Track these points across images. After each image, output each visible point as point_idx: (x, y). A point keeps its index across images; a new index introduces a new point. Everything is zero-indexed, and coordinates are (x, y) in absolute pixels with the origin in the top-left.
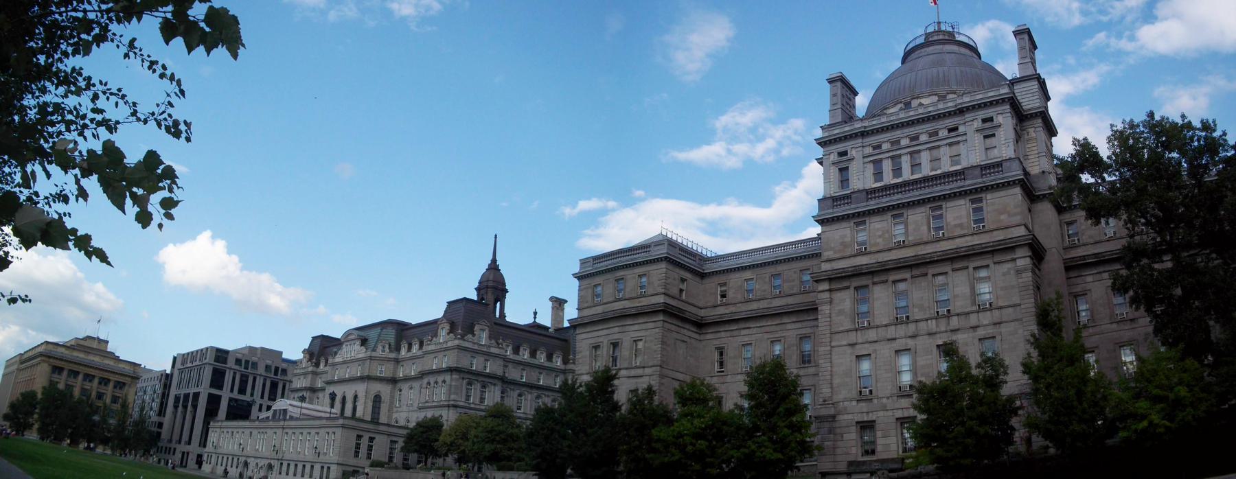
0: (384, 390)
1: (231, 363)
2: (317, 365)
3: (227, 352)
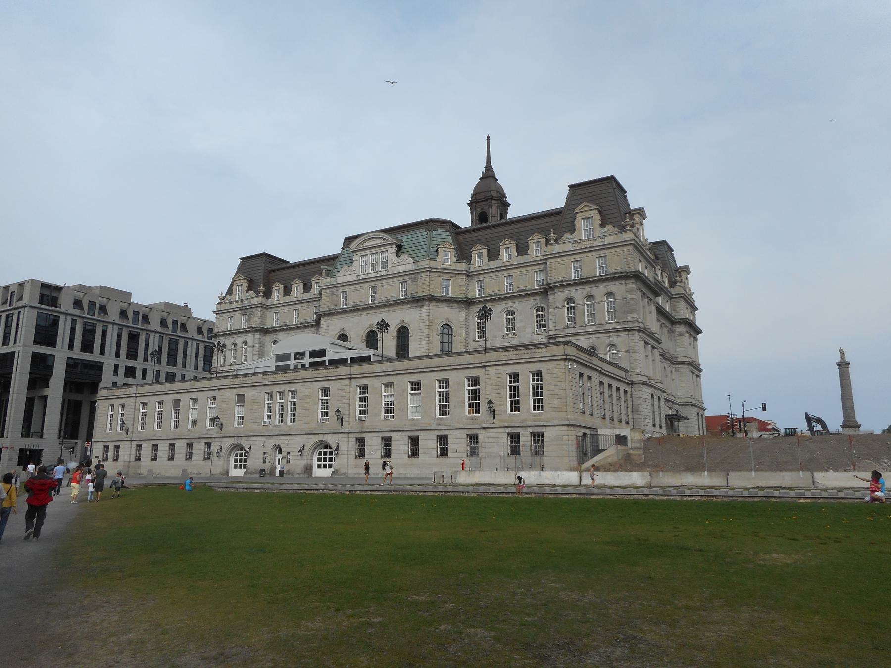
1: (66, 304)
2: (268, 294)
3: (59, 289)
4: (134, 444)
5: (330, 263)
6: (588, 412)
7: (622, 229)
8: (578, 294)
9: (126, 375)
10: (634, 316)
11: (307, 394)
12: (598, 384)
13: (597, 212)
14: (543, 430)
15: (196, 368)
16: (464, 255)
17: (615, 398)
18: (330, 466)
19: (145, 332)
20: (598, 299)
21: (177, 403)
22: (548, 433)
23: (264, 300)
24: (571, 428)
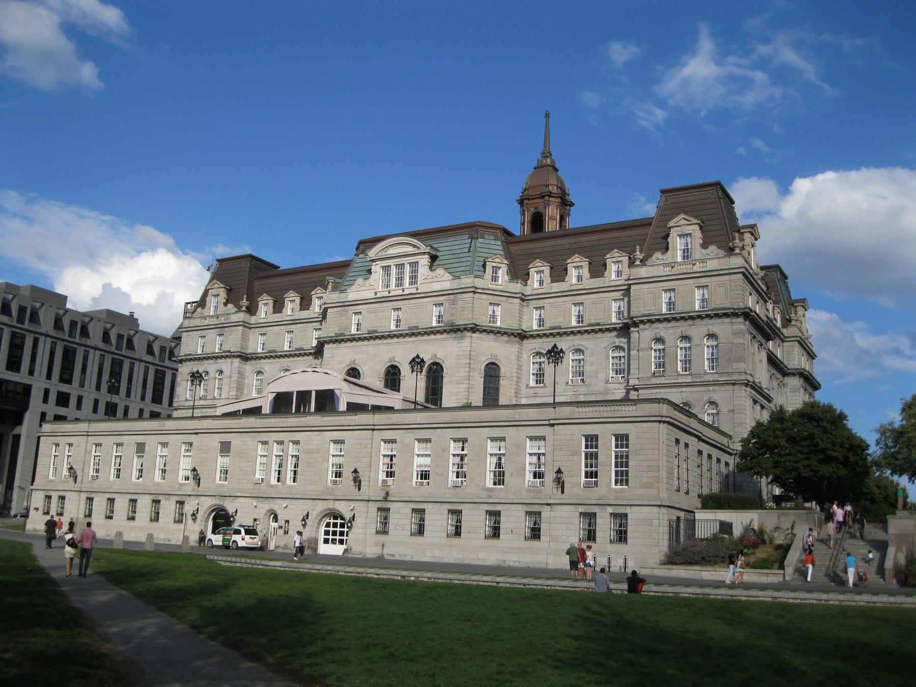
2: (252, 310)
4: (84, 496)
5: (336, 272)
6: (684, 488)
7: (731, 251)
8: (668, 331)
9: (58, 404)
10: (741, 366)
11: (314, 447)
12: (696, 454)
13: (697, 227)
14: (628, 510)
15: (143, 398)
16: (519, 273)
17: (705, 468)
18: (341, 542)
19: (83, 349)
20: (695, 341)
21: (141, 448)
22: (633, 514)
23: (248, 316)
24: (664, 510)
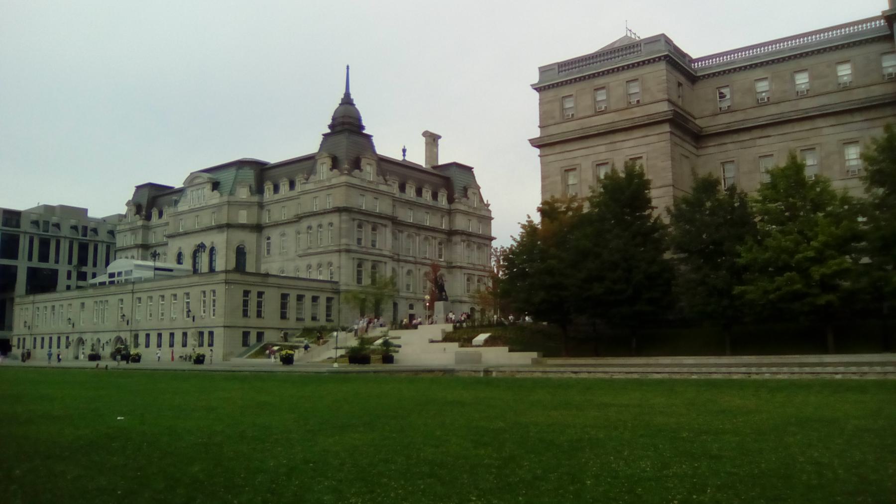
0: (249, 239)
2: (148, 217)
8: (314, 222)
